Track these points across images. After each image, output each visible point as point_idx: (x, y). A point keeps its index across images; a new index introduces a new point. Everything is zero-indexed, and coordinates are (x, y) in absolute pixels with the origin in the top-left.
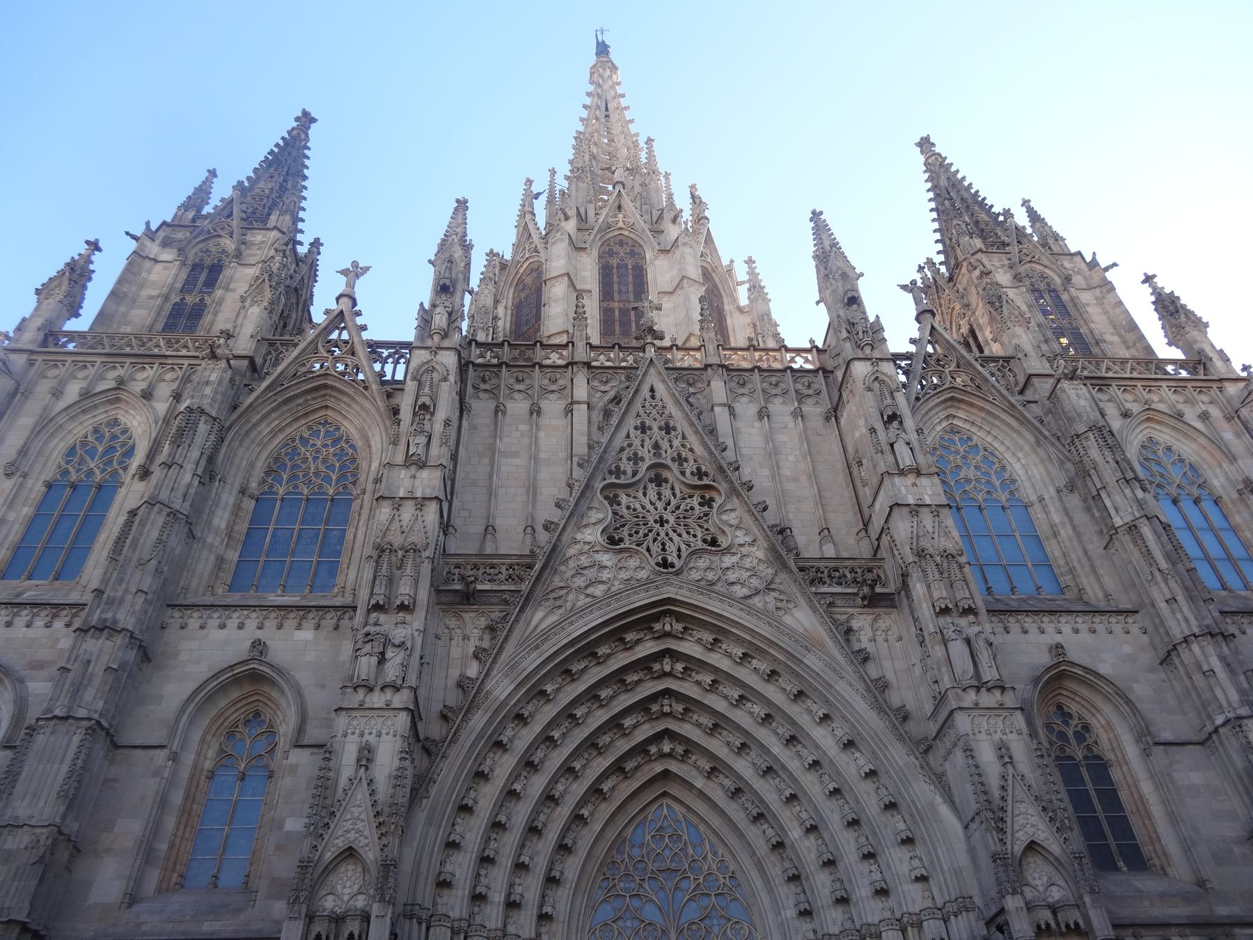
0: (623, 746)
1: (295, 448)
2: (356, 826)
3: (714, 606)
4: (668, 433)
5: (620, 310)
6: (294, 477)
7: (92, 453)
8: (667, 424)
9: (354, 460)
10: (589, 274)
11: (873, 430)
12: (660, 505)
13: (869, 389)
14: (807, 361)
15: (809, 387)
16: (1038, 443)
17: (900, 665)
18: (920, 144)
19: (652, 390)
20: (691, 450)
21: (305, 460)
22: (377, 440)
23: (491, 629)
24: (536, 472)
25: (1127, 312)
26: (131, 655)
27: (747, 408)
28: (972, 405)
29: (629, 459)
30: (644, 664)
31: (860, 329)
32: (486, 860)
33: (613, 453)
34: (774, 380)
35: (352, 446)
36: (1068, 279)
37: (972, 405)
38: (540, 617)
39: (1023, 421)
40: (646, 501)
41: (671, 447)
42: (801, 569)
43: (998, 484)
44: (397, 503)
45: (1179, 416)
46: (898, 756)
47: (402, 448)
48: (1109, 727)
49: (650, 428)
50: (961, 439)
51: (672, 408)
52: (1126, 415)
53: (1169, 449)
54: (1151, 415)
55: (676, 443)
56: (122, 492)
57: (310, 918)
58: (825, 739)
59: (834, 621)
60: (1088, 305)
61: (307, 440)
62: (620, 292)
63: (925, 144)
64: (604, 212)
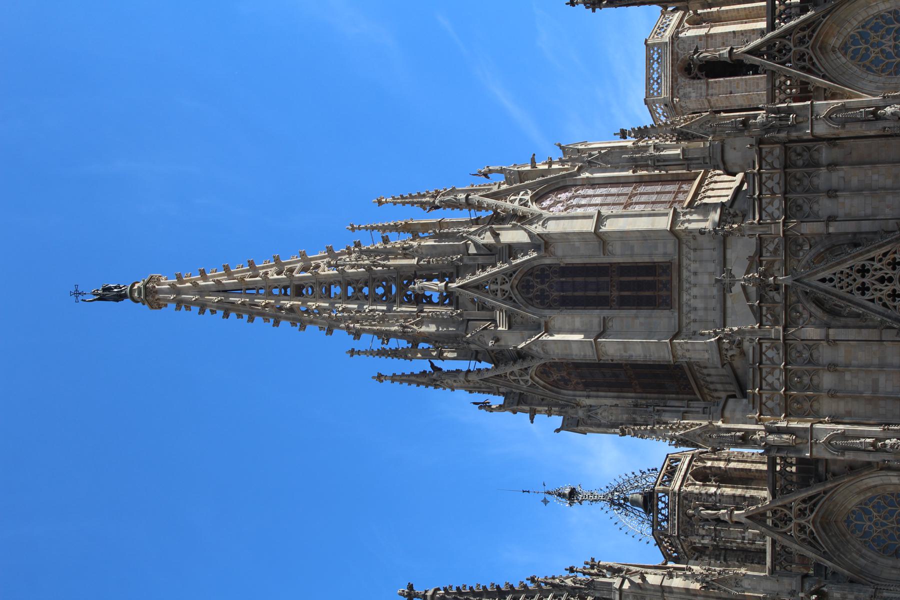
1: (873, 540)
4: (868, 271)
5: (621, 290)
8: (858, 271)
9: (884, 498)
13: (843, 126)
14: (771, 152)
15: (799, 155)
20: (885, 255)
21: (885, 532)
22: (874, 480)
27: (825, 206)
28: (827, 33)
29: (894, 300)
31: (778, 123)
34: (796, 183)
35: (871, 499)
37: (827, 33)
41: (881, 269)
49: (863, 284)
50: (853, 44)
51: (844, 267)
55: (877, 265)
61: (865, 532)
62: (598, 290)
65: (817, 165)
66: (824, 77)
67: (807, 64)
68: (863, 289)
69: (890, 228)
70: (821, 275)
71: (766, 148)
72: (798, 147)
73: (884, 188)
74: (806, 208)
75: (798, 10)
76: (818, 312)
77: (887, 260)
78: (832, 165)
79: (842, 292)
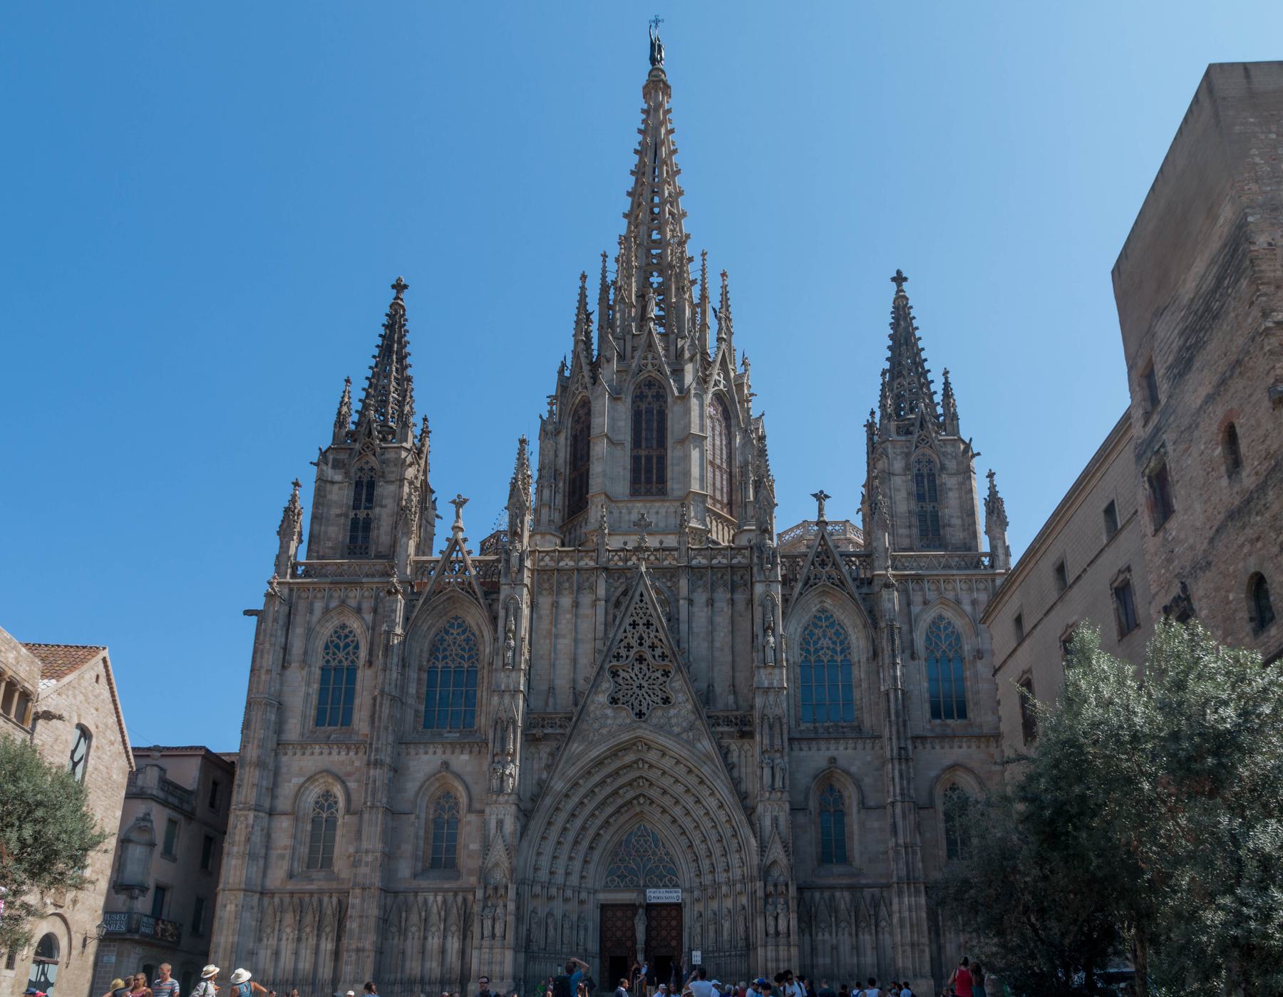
0: (620, 802)
2: (499, 853)
3: (662, 740)
6: (445, 657)
7: (337, 646)
10: (622, 424)
11: (754, 637)
12: (640, 676)
16: (865, 626)
17: (749, 770)
18: (893, 279)
19: (642, 595)
22: (487, 635)
23: (552, 754)
24: (576, 648)
25: (972, 499)
26: (392, 774)
27: (701, 597)
30: (628, 767)
32: (555, 858)
33: (616, 643)
35: (473, 634)
36: (943, 467)
38: (576, 747)
39: (860, 610)
40: (631, 673)
42: (709, 717)
43: (839, 649)
44: (502, 693)
45: (958, 602)
46: (739, 817)
47: (501, 657)
48: (850, 797)
51: (651, 610)
52: (925, 603)
53: (949, 623)
54: (944, 602)
55: (652, 635)
56: (360, 674)
57: (485, 888)
58: (712, 803)
59: (720, 747)
60: (950, 489)
63: (899, 279)
64: (637, 354)
65: (733, 591)
66: (801, 594)
67: (811, 582)
68: (634, 625)
69: (682, 646)
70: (645, 593)
71: (747, 553)
72: (747, 577)
73: (712, 642)
74: (701, 583)
75: (854, 575)
76: (618, 593)
77: (657, 642)
78: (732, 602)
79: (632, 609)
